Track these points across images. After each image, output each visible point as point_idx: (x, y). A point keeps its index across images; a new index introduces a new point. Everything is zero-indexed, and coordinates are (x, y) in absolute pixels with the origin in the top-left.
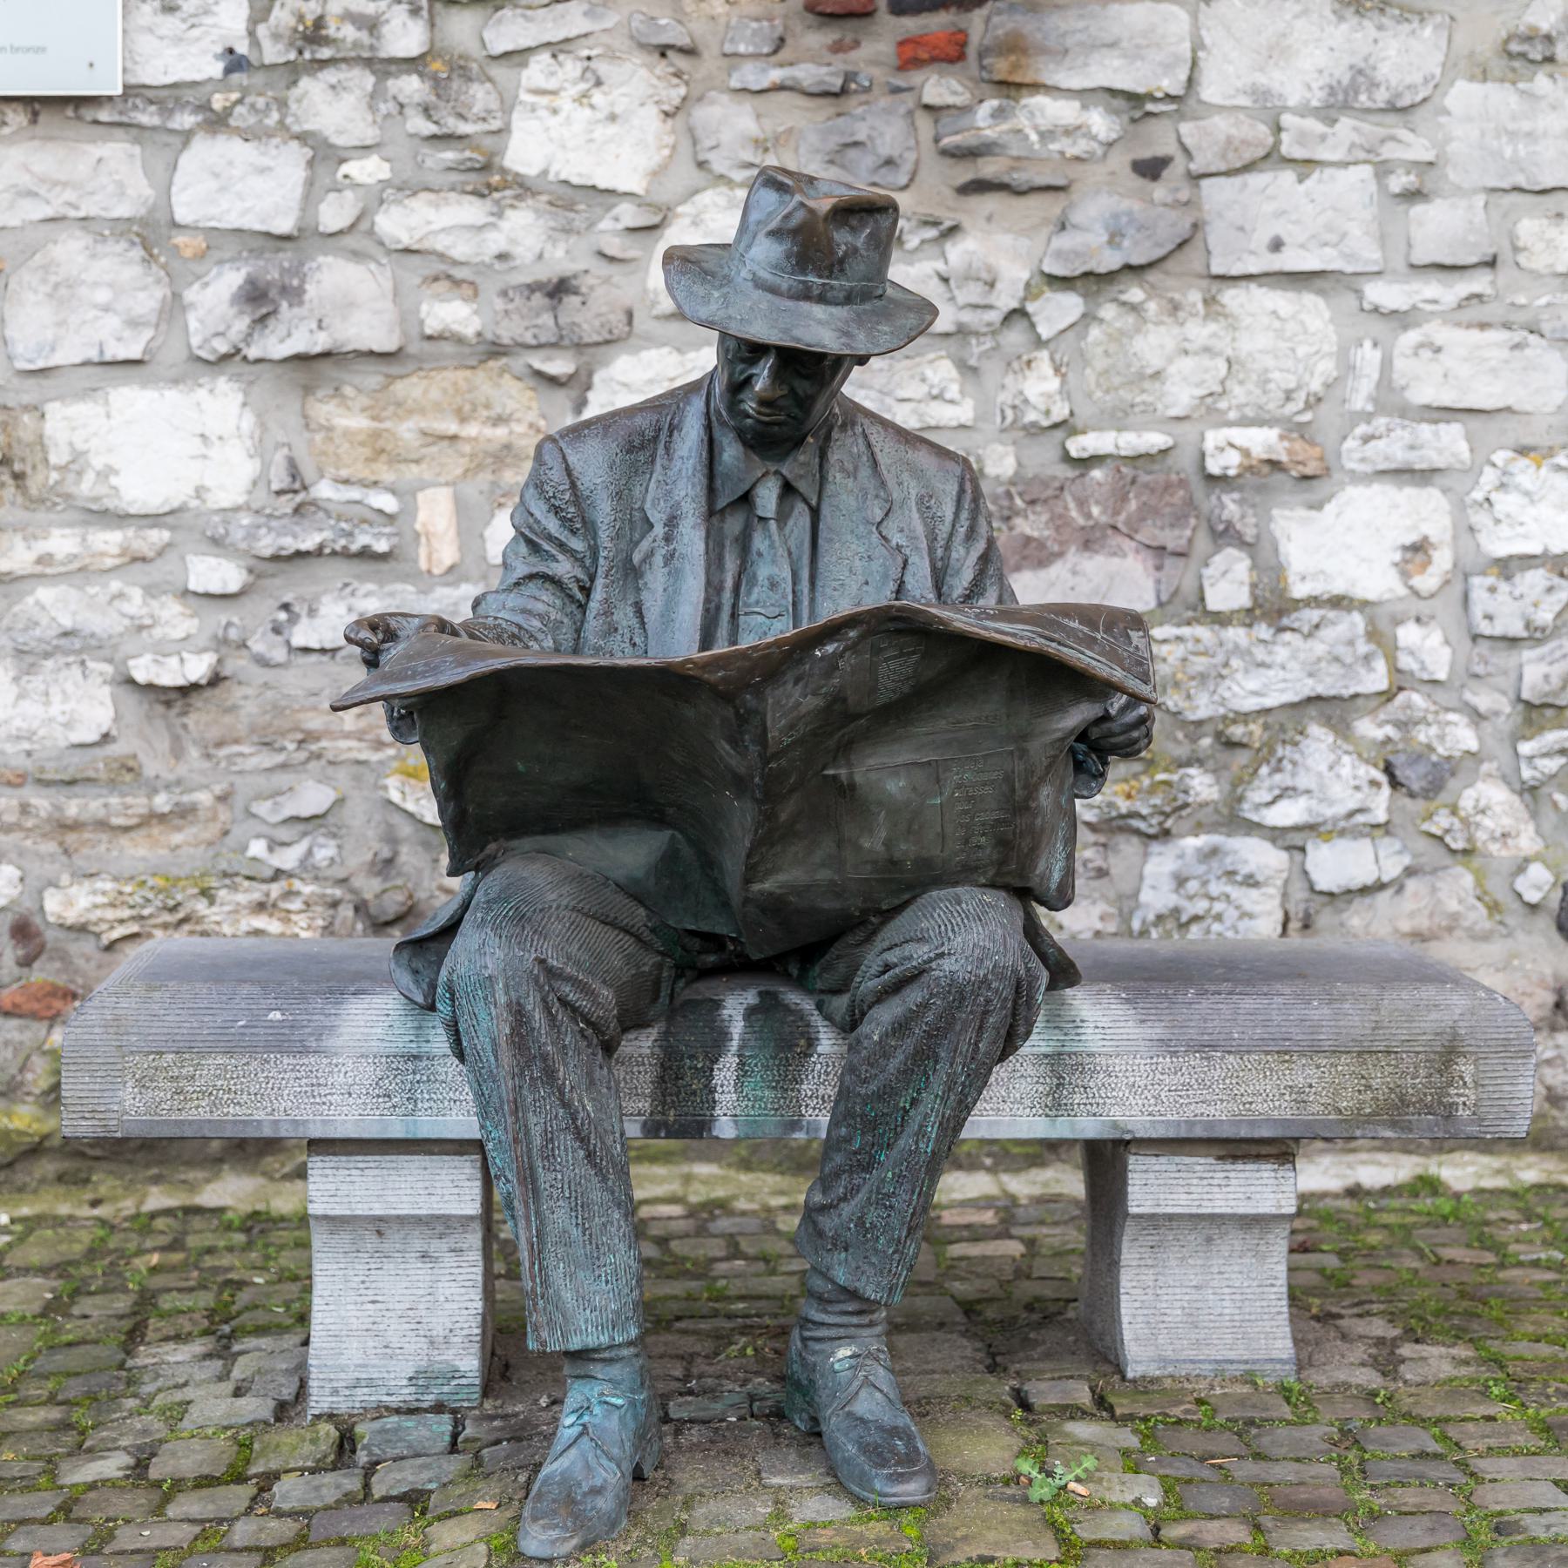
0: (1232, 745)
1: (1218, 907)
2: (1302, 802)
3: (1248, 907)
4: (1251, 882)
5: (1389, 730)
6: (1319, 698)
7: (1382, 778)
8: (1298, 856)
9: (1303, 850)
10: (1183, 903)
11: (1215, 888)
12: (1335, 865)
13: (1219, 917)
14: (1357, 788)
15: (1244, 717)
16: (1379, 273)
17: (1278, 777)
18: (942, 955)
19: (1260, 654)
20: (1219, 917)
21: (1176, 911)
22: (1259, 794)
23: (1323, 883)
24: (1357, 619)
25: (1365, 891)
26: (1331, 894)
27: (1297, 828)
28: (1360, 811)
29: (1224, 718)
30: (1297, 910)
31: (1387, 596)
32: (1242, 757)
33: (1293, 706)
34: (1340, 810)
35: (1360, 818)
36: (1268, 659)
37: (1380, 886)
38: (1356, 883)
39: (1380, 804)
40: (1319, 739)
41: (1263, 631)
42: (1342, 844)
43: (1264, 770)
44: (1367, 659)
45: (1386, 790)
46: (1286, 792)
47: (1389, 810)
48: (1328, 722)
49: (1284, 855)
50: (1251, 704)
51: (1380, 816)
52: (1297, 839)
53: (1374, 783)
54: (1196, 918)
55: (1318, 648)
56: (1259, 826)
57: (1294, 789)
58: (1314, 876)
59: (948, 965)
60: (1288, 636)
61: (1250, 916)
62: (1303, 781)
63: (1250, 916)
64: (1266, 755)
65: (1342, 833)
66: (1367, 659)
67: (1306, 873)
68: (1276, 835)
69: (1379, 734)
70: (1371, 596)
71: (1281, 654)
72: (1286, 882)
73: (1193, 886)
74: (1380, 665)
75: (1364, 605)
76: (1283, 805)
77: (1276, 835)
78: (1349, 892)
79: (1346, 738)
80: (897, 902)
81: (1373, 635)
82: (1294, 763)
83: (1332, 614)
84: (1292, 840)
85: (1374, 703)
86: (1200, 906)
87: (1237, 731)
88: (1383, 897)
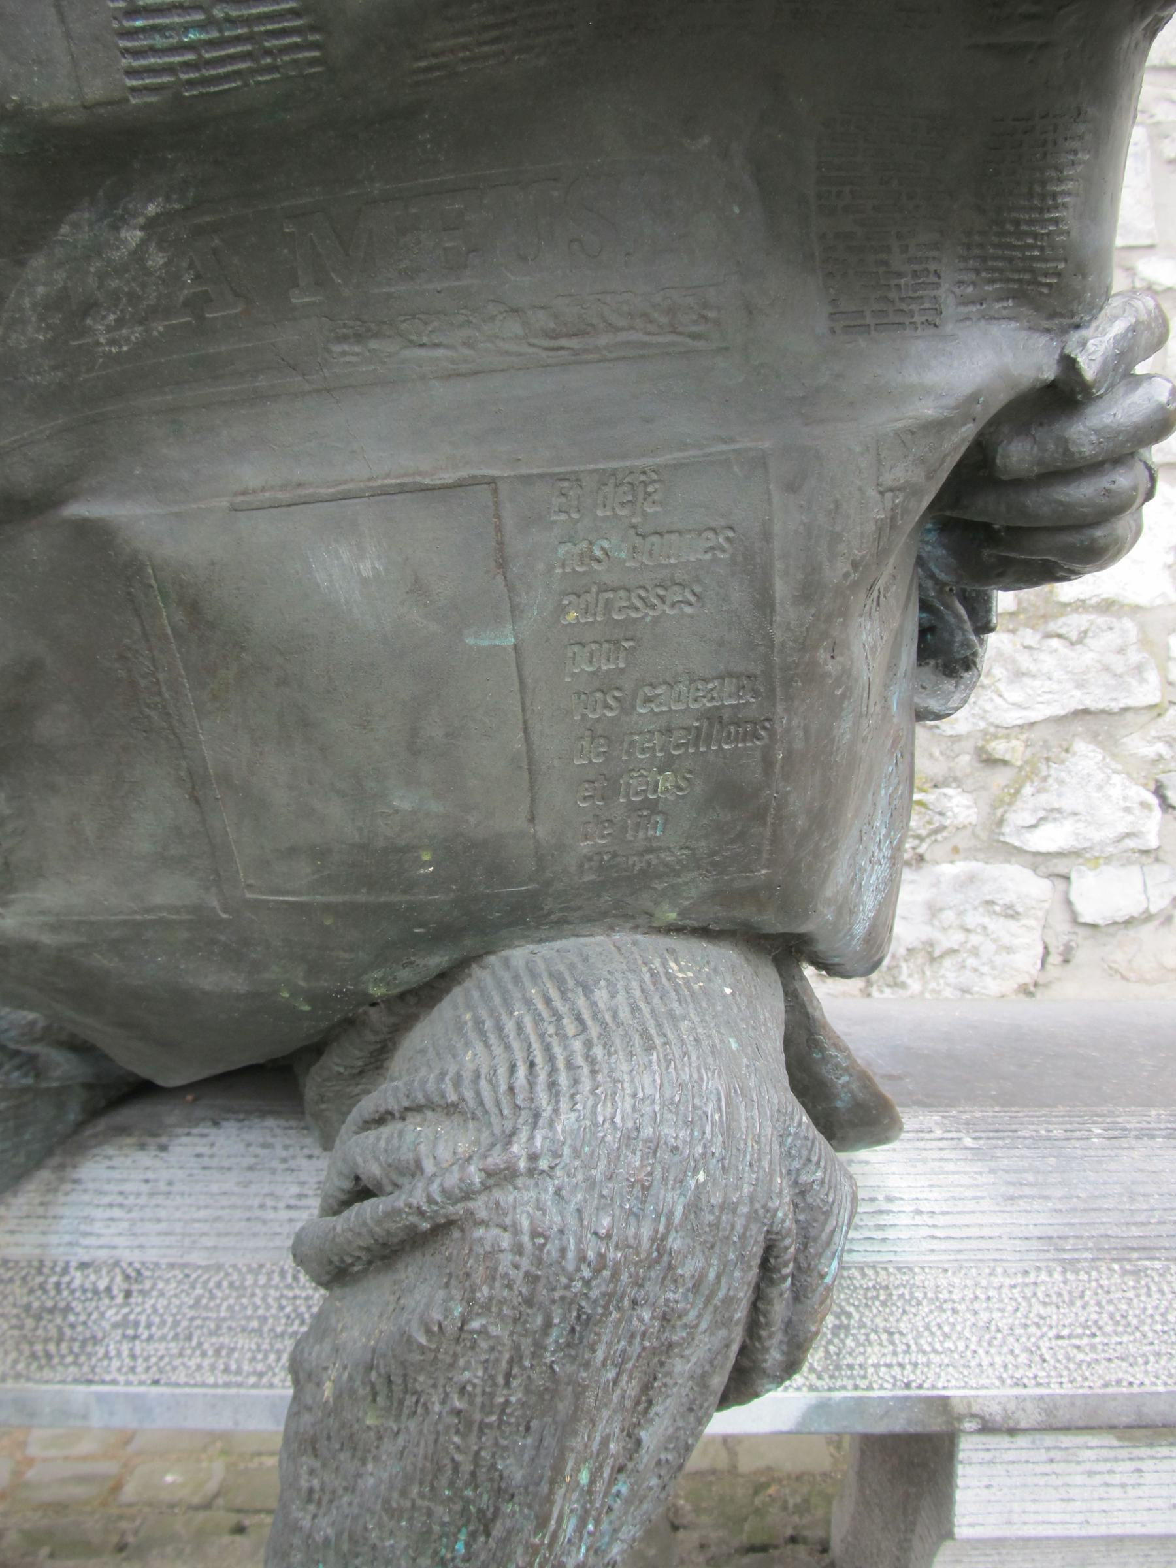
0: (990, 761)
1: (975, 939)
2: (1068, 825)
3: (1006, 940)
4: (1011, 913)
5: (1161, 748)
6: (1086, 712)
7: (1154, 801)
8: (1061, 885)
9: (1067, 878)
10: (937, 935)
11: (973, 919)
12: (1102, 894)
13: (975, 952)
14: (1127, 810)
15: (1009, 732)
16: (1151, 247)
17: (1043, 799)
18: (504, 1176)
19: (1025, 662)
20: (975, 952)
21: (931, 944)
22: (1020, 816)
23: (1088, 914)
24: (1128, 624)
25: (1129, 922)
26: (1094, 926)
27: (1060, 854)
28: (1128, 835)
29: (985, 733)
30: (1056, 947)
31: (1159, 602)
32: (1000, 778)
33: (1059, 720)
34: (1109, 833)
35: (1130, 843)
36: (1033, 668)
37: (1147, 917)
38: (1121, 916)
39: (1152, 827)
40: (1086, 756)
41: (1030, 637)
42: (1109, 871)
43: (1028, 790)
44: (1139, 669)
45: (1157, 812)
46: (1053, 814)
47: (1160, 835)
48: (1094, 738)
49: (1046, 884)
50: (1014, 717)
51: (1153, 842)
52: (1061, 866)
53: (1144, 805)
54: (952, 952)
55: (1086, 657)
56: (1020, 851)
57: (1059, 811)
58: (1080, 907)
59: (524, 1204)
60: (1055, 643)
61: (1009, 950)
62: (1067, 804)
63: (1009, 950)
64: (1030, 772)
65: (1108, 860)
66: (1139, 669)
67: (1069, 903)
68: (1038, 861)
69: (1150, 751)
70: (1143, 601)
71: (1048, 662)
72: (1048, 912)
73: (949, 916)
74: (1153, 677)
75: (1136, 609)
76: (1047, 829)
77: (1038, 861)
78: (1115, 923)
79: (1114, 756)
80: (407, 977)
81: (1145, 642)
82: (1061, 782)
83: (1101, 620)
84: (1055, 867)
85: (1144, 718)
86: (954, 939)
87: (999, 748)
88: (1146, 932)
